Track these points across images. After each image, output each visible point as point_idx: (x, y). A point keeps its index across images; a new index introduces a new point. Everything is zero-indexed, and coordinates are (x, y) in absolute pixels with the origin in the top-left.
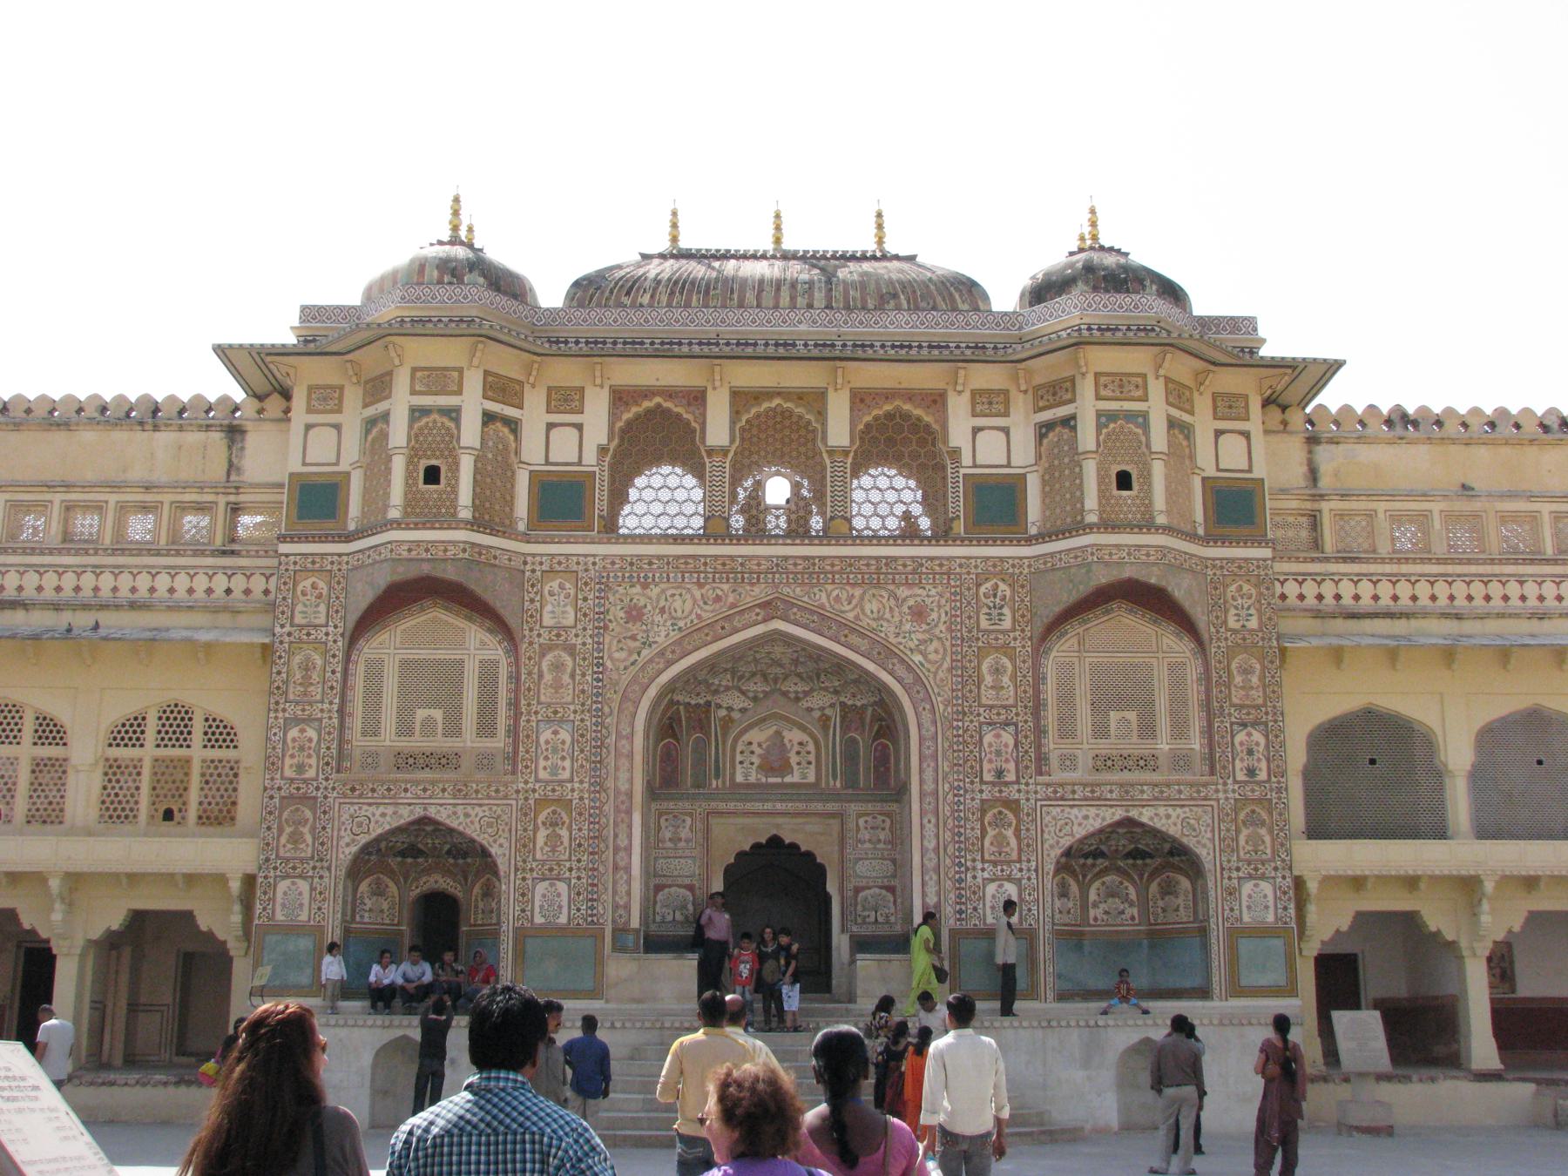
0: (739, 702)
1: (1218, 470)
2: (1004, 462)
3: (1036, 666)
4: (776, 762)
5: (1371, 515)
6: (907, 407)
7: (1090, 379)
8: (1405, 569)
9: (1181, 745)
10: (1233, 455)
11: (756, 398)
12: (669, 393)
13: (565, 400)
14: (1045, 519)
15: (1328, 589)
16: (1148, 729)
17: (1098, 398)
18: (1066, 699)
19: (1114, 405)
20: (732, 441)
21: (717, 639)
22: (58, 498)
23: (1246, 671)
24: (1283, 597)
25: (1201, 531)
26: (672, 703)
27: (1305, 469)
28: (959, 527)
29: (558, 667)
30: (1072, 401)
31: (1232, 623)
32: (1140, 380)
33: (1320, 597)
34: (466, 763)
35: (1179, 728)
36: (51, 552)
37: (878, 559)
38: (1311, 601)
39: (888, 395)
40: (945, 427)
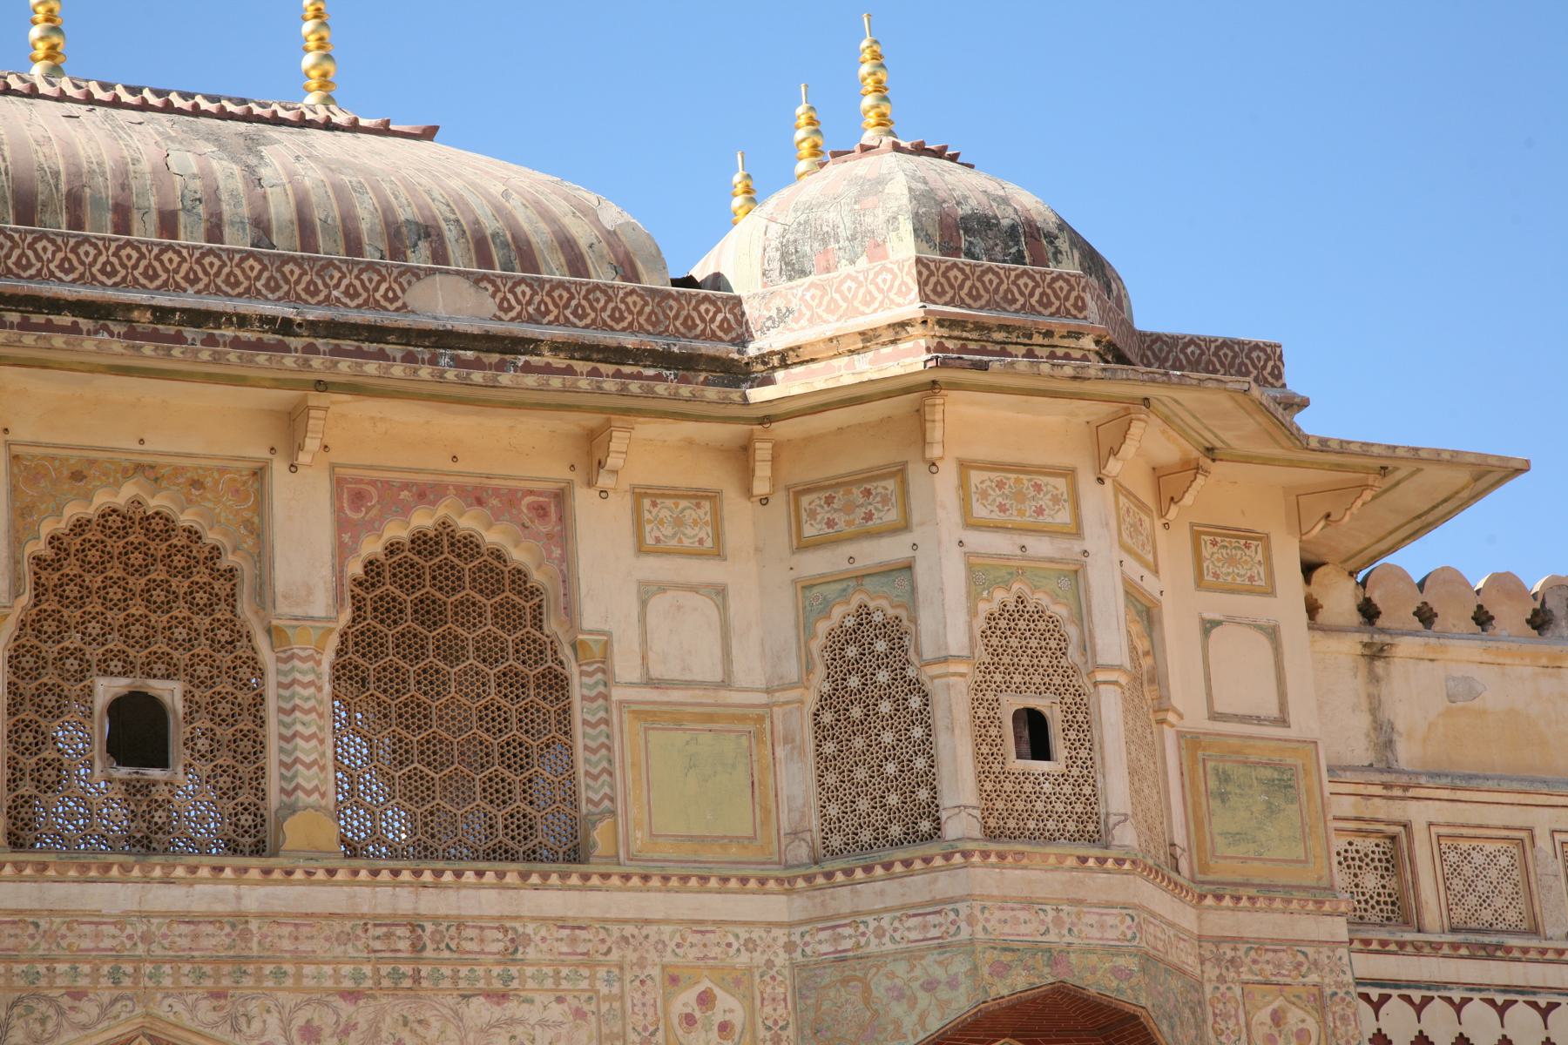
1: (1215, 716)
2: (718, 677)
5: (1523, 841)
6: (467, 523)
7: (947, 476)
10: (1244, 680)
11: (77, 476)
14: (830, 826)
17: (970, 523)
19: (1002, 544)
27: (1363, 721)
30: (904, 526)
32: (1061, 484)
37: (414, 924)
39: (426, 494)
40: (568, 580)
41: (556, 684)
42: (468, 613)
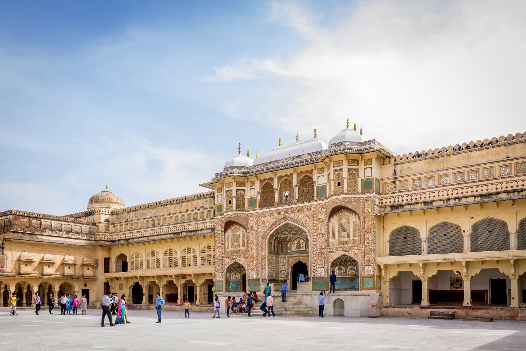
0: (291, 236)
3: (328, 225)
4: (299, 247)
8: (414, 192)
9: (355, 238)
12: (268, 179)
13: (253, 184)
15: (396, 200)
16: (349, 236)
18: (334, 231)
20: (278, 186)
21: (278, 225)
22: (192, 213)
23: (368, 221)
24: (386, 203)
25: (360, 192)
26: (277, 238)
28: (315, 198)
29: (253, 234)
31: (366, 211)
33: (394, 202)
34: (241, 252)
35: (355, 235)
36: (192, 222)
38: (392, 203)
39: (303, 173)
41: (313, 186)
42: (307, 181)
